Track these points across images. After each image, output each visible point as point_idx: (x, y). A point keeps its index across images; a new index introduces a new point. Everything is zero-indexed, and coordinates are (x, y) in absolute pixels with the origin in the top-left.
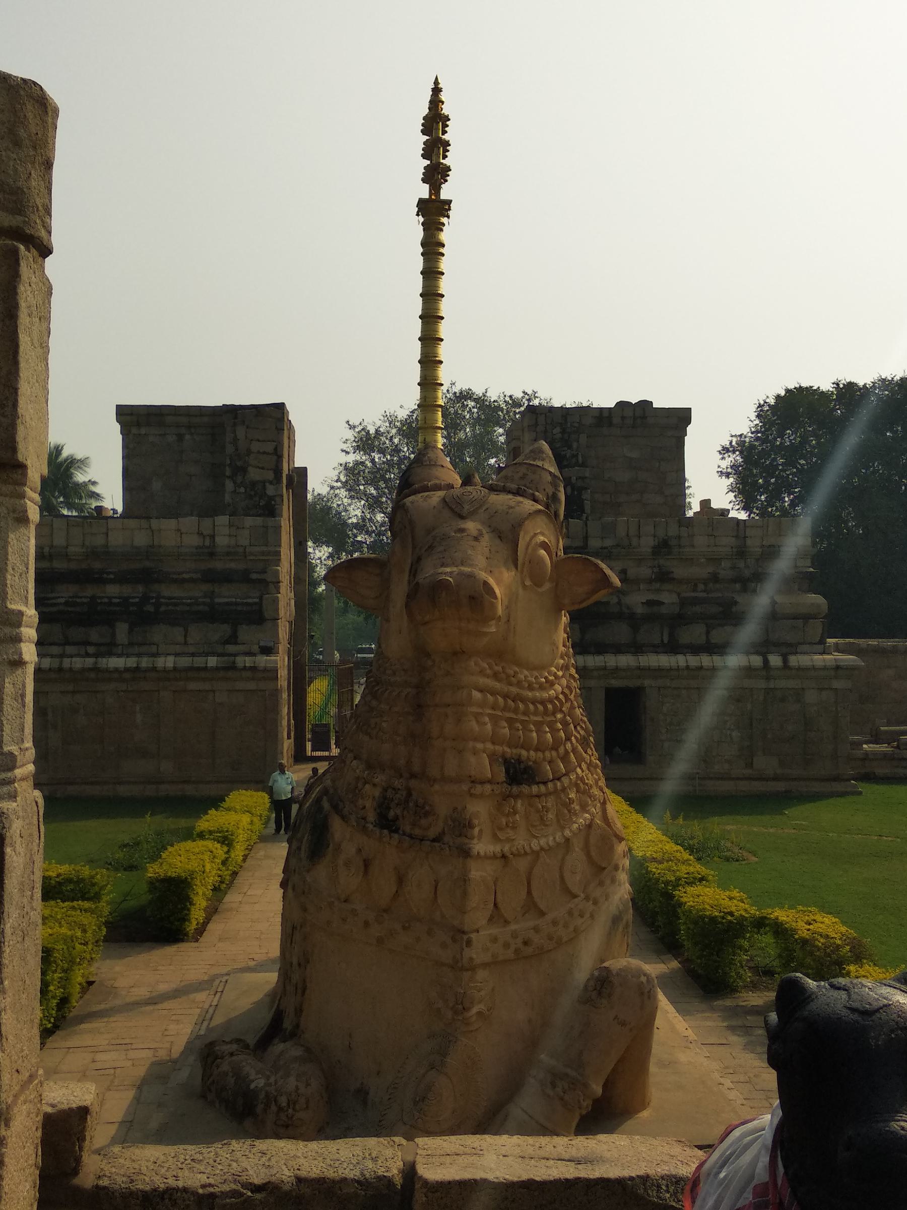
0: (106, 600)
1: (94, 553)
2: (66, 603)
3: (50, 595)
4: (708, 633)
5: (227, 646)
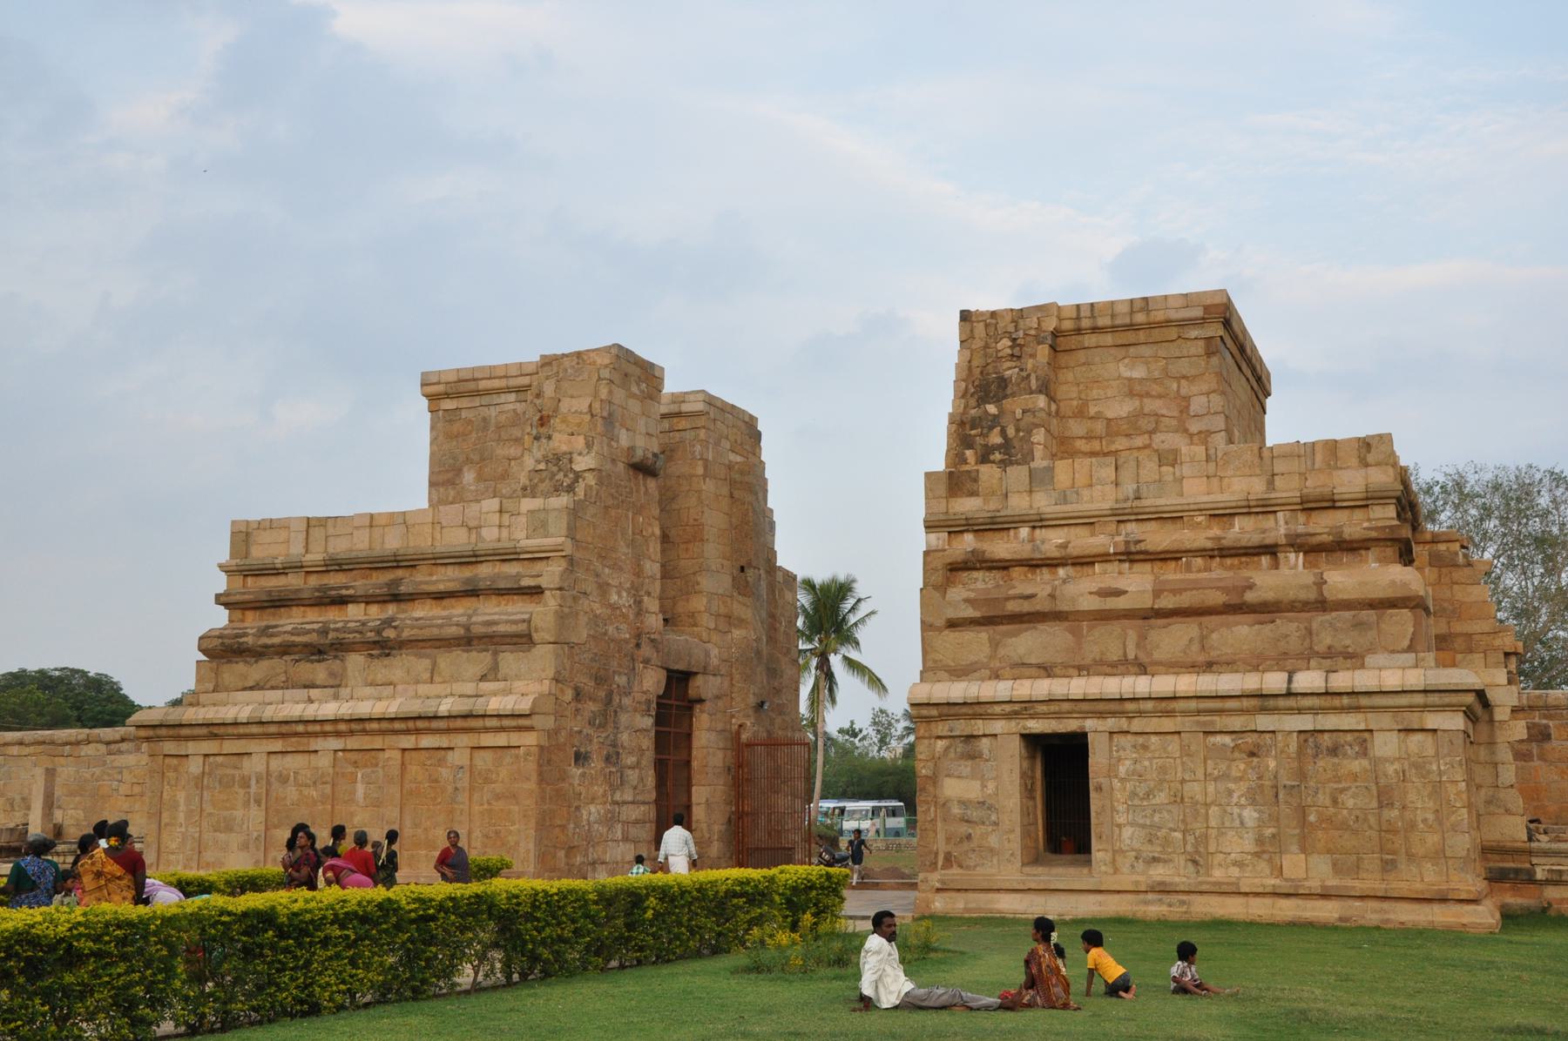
0: (340, 625)
1: (336, 565)
3: (281, 622)
4: (1203, 638)
5: (481, 684)
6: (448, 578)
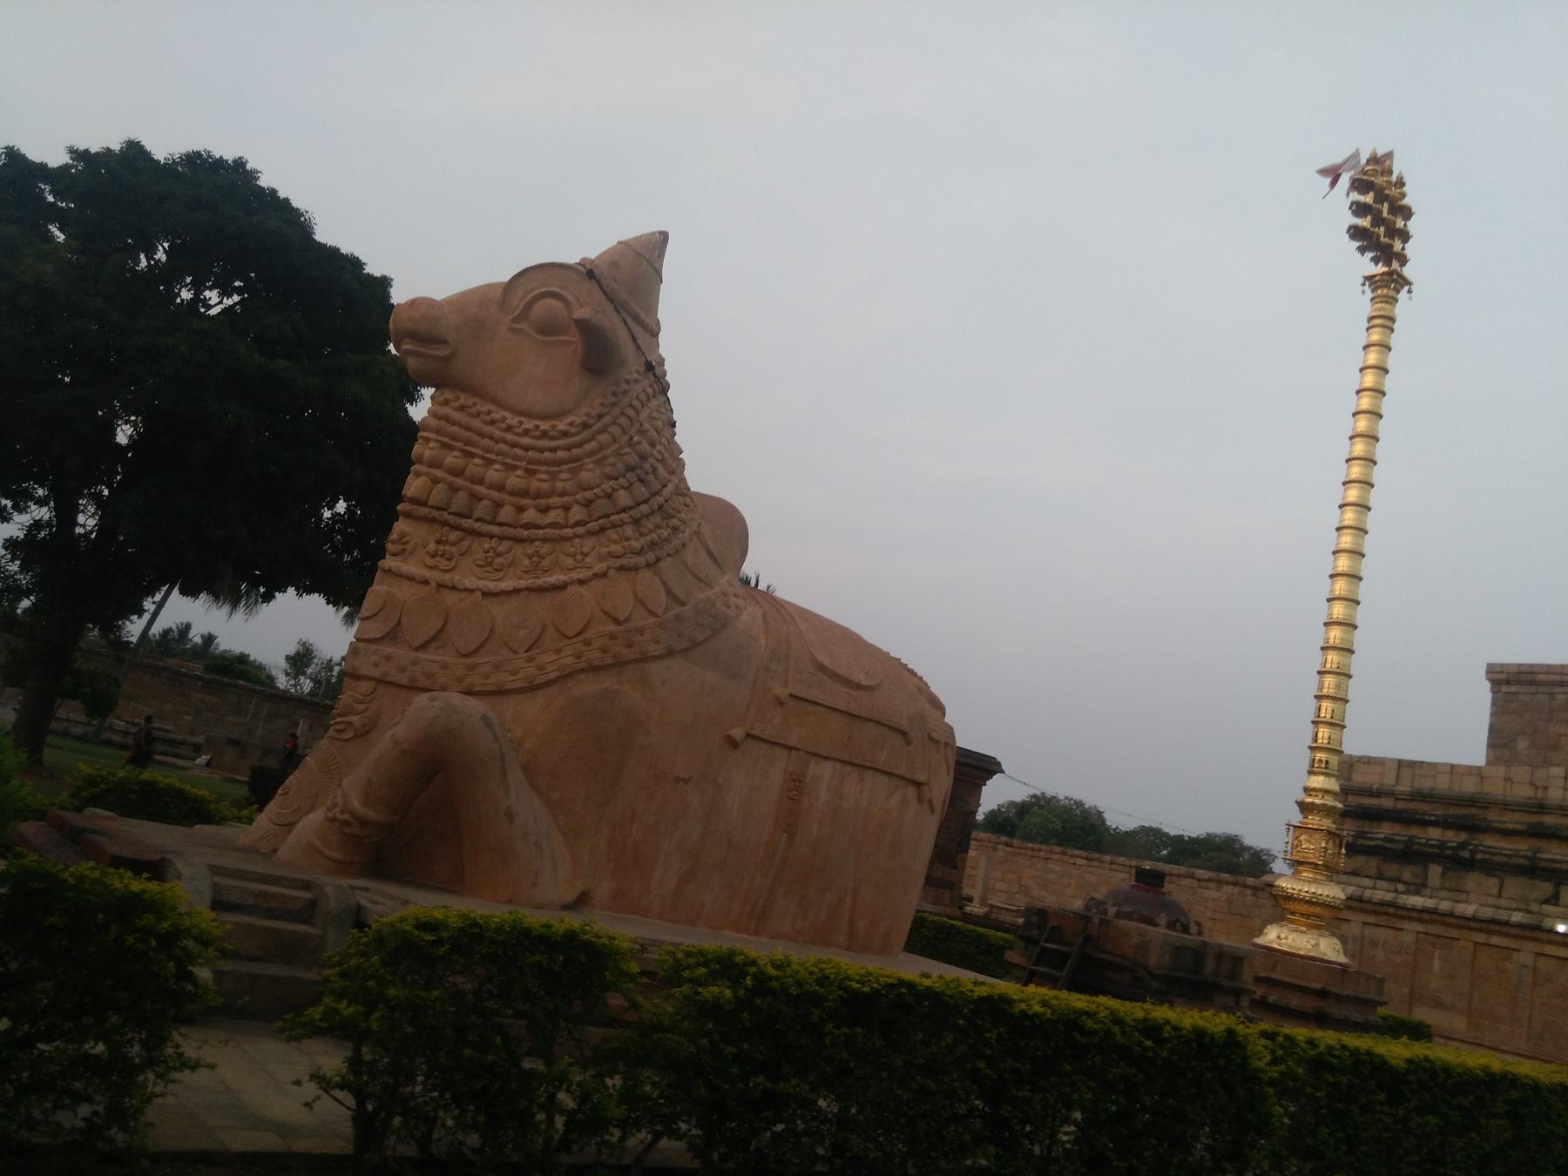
0: (1423, 841)
1: (1419, 796)
2: (1385, 840)
6: (1514, 820)
